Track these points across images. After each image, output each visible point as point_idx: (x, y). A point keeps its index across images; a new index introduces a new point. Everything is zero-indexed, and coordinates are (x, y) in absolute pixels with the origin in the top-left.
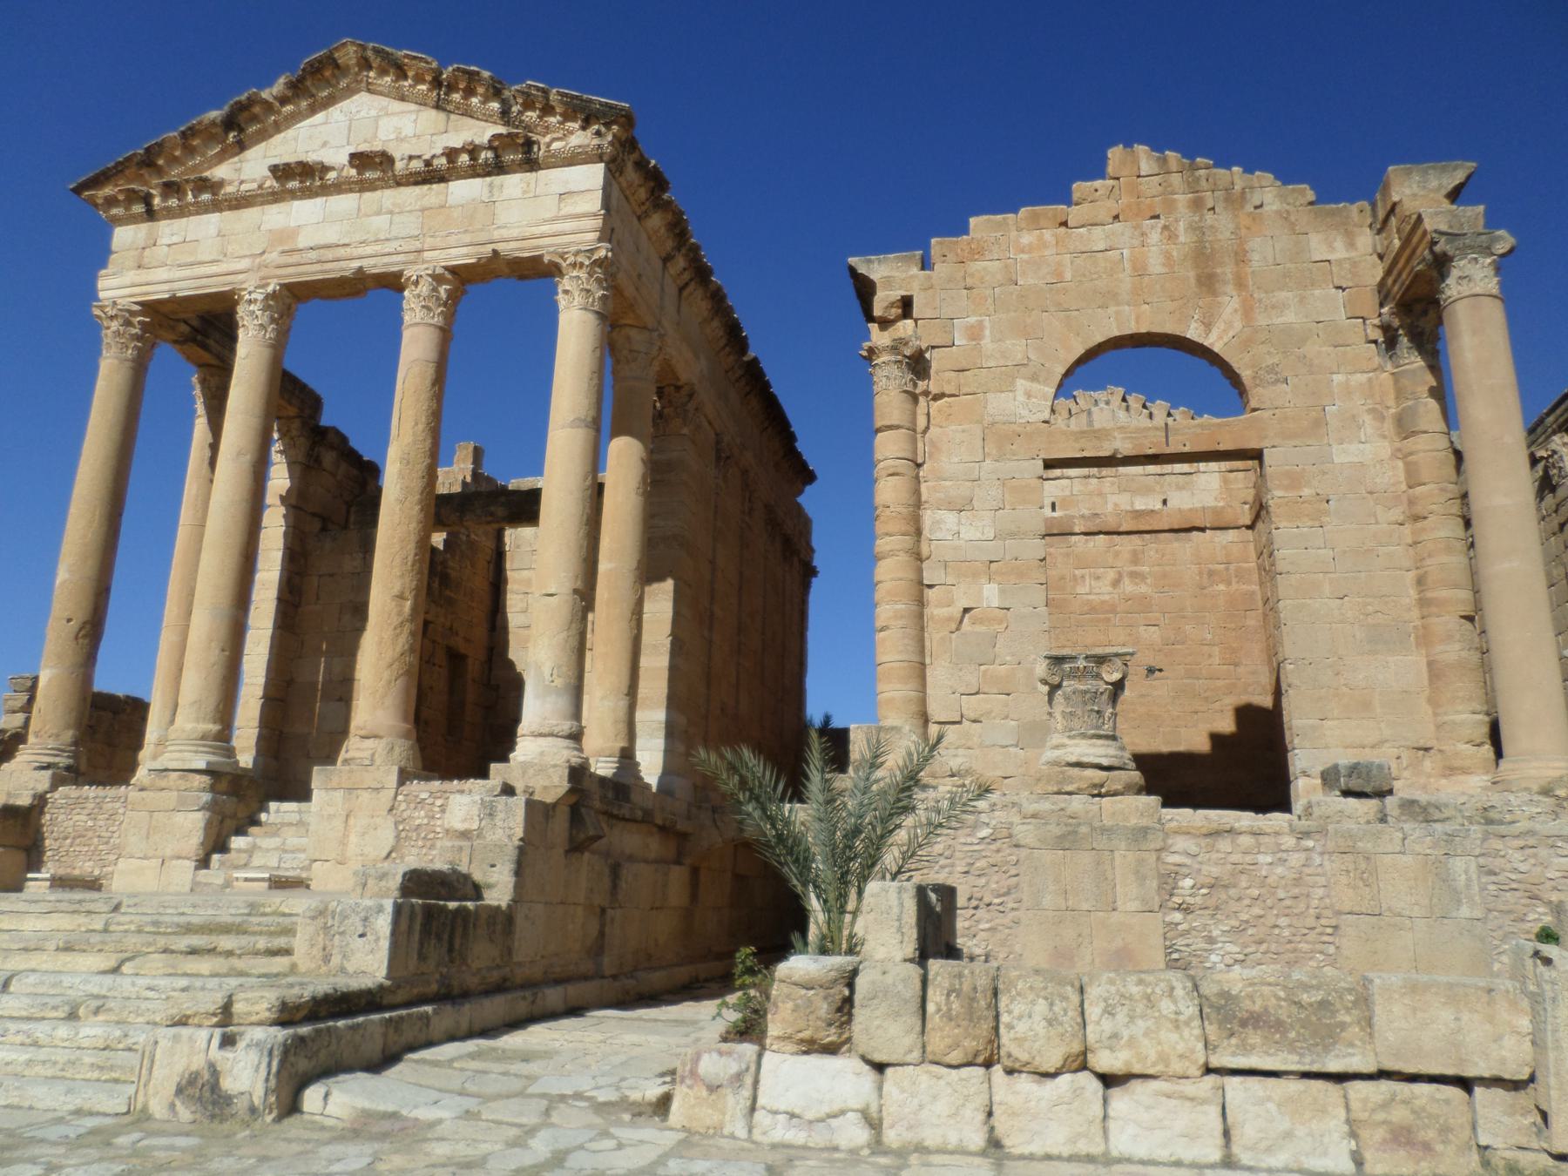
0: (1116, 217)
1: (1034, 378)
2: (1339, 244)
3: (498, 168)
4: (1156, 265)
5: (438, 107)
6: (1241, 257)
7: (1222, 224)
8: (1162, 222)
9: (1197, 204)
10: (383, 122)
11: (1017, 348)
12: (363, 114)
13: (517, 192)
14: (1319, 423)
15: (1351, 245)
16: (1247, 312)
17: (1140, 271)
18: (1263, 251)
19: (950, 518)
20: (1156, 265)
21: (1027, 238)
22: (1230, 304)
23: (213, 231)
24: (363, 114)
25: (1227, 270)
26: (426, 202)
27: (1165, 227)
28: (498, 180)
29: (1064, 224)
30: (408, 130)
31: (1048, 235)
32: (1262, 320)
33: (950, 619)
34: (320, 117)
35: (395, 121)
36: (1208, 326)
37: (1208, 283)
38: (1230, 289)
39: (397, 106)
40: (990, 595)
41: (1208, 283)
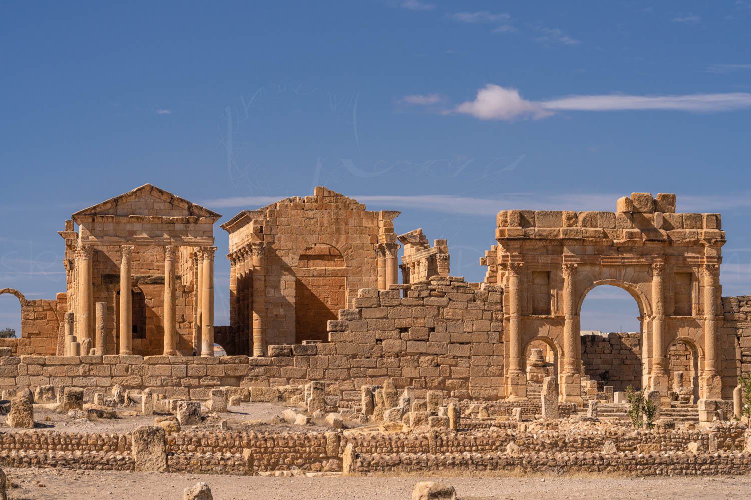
0: (317, 209)
1: (294, 254)
2: (370, 222)
3: (188, 222)
4: (326, 224)
5: (170, 203)
6: (347, 224)
7: (343, 212)
8: (328, 211)
9: (337, 207)
10: (155, 204)
11: (290, 245)
12: (149, 201)
13: (193, 229)
14: (361, 270)
15: (373, 223)
16: (347, 239)
17: (322, 225)
18: (352, 222)
19: (272, 291)
20: (326, 224)
21: (294, 212)
22: (343, 237)
23: (111, 228)
24: (149, 201)
25: (343, 227)
26: (169, 228)
27: (329, 213)
28: (188, 225)
29: (303, 209)
30: (162, 207)
31: (299, 211)
32: (350, 242)
33: (272, 317)
34: (137, 200)
35: (159, 204)
36: (337, 243)
37: (338, 231)
38: (343, 232)
39: (158, 200)
40: (282, 311)
41: (338, 231)
